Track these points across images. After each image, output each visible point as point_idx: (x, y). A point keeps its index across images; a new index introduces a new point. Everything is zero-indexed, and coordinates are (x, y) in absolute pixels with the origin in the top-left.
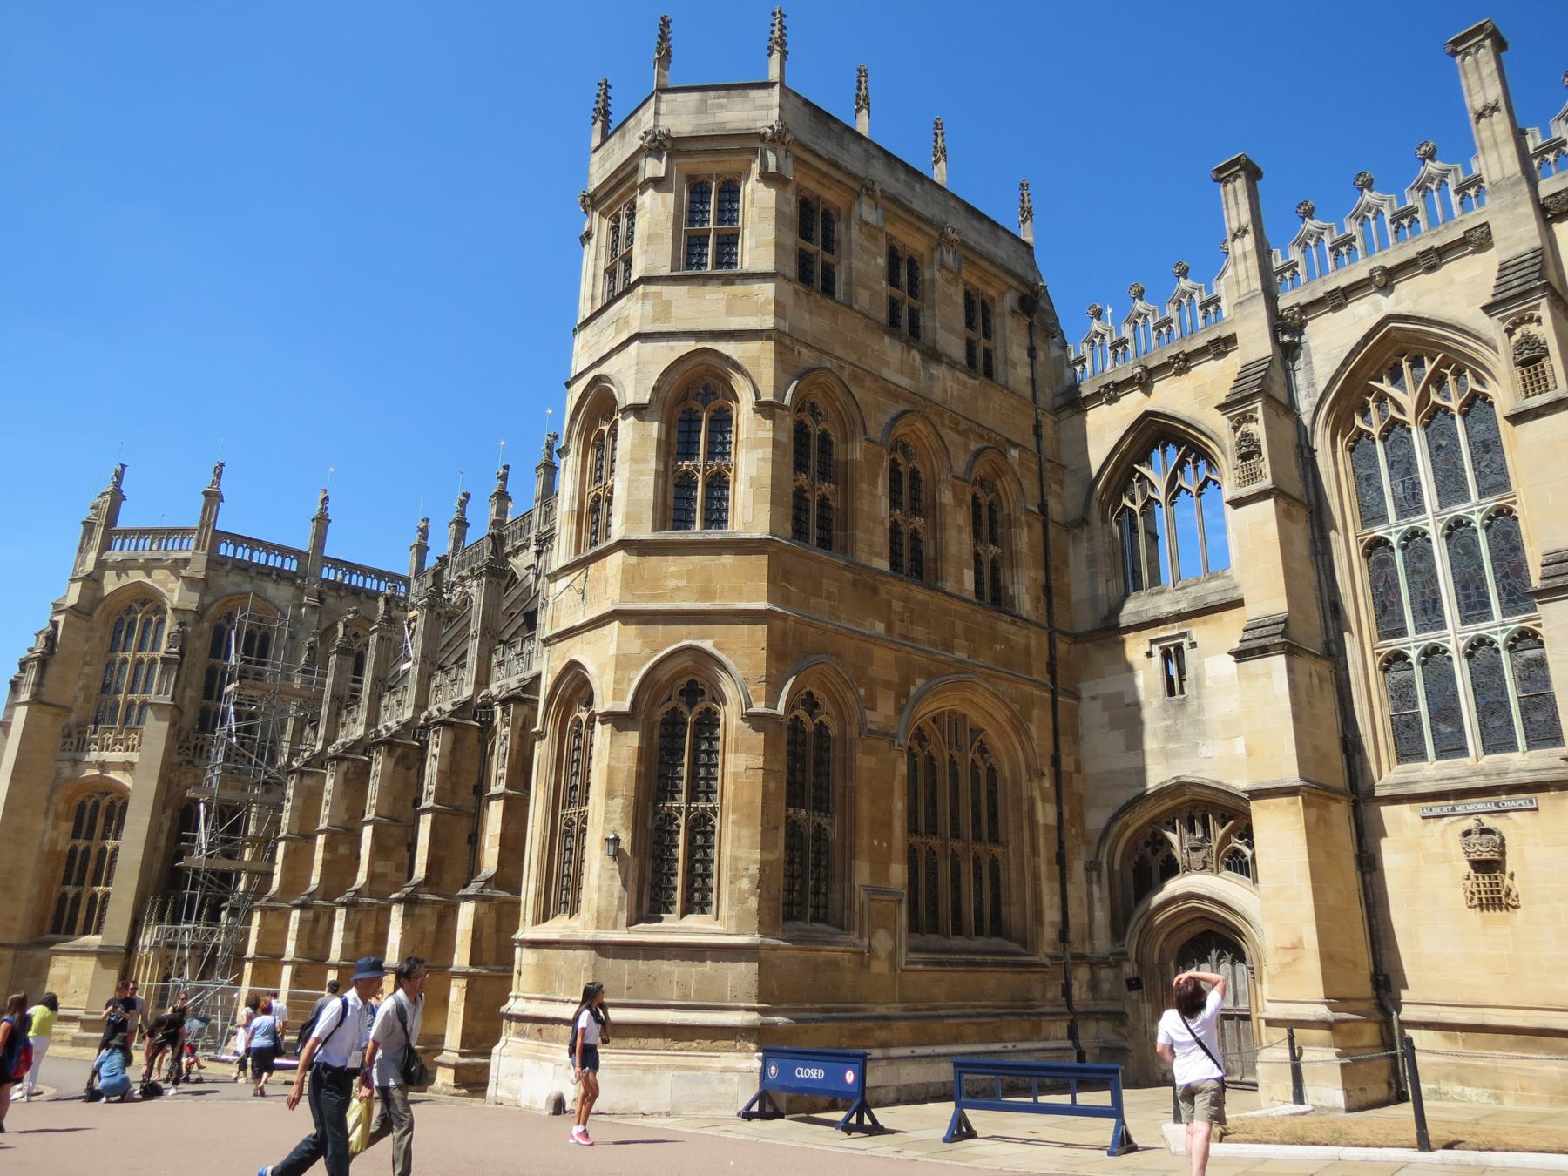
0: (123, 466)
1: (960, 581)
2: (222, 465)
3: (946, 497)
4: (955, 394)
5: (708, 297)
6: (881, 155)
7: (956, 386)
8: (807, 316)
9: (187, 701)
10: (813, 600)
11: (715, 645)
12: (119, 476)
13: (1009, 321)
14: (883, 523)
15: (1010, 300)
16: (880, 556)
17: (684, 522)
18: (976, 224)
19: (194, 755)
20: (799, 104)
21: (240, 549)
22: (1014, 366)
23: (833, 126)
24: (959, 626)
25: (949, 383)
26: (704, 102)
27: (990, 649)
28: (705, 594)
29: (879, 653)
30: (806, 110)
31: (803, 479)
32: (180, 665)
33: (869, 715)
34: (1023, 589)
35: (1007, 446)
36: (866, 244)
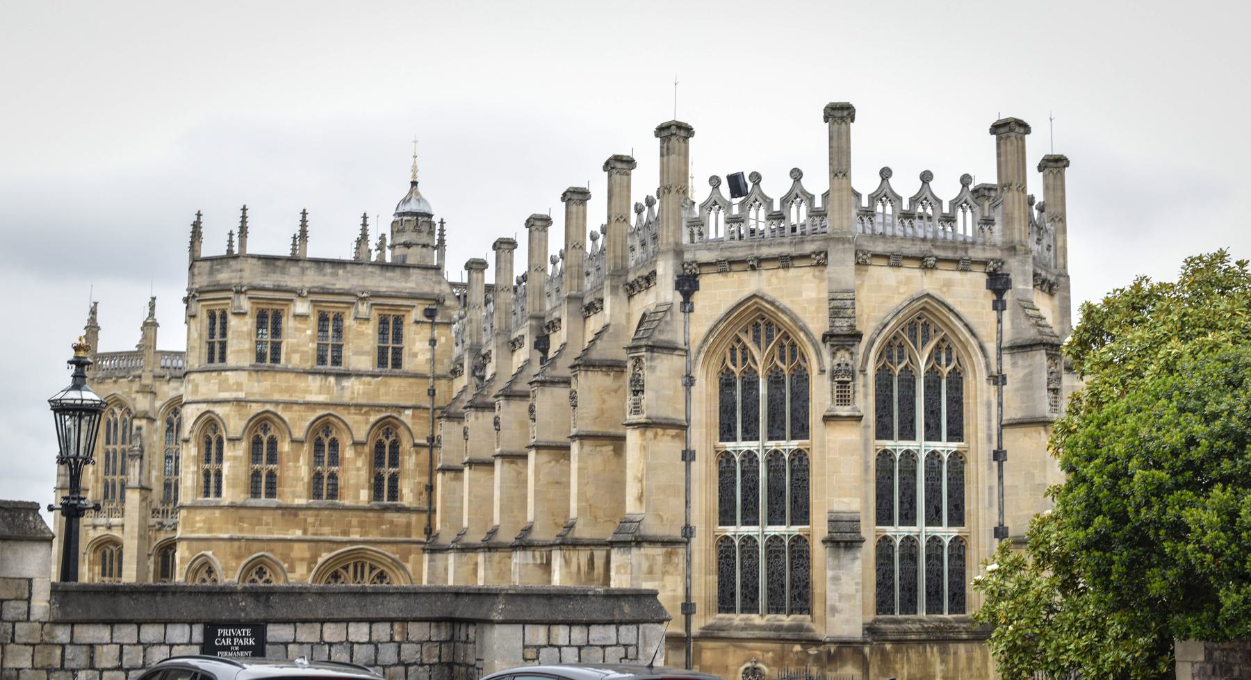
0: (96, 304)
1: (357, 497)
2: (154, 299)
3: (348, 453)
4: (361, 392)
5: (212, 381)
6: (313, 264)
7: (361, 387)
8: (256, 384)
9: (153, 480)
10: (257, 528)
11: (213, 553)
12: (93, 312)
13: (414, 328)
14: (303, 480)
15: (417, 313)
16: (300, 497)
17: (207, 494)
18: (389, 274)
19: (163, 517)
20: (254, 261)
21: (175, 361)
22: (415, 355)
23: (279, 263)
24: (355, 521)
25: (356, 388)
26: (211, 267)
27: (377, 529)
28: (210, 530)
29: (296, 546)
30: (260, 263)
31: (257, 466)
32: (141, 458)
33: (290, 575)
34: (408, 494)
35: (402, 410)
36: (299, 326)
